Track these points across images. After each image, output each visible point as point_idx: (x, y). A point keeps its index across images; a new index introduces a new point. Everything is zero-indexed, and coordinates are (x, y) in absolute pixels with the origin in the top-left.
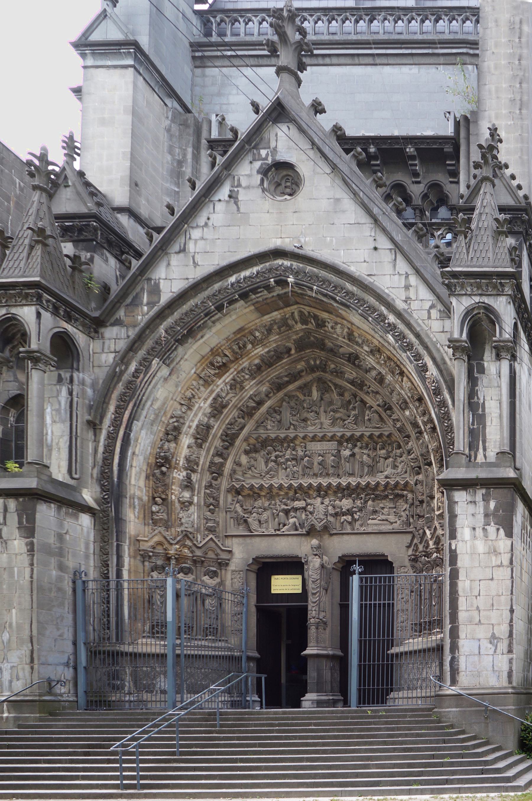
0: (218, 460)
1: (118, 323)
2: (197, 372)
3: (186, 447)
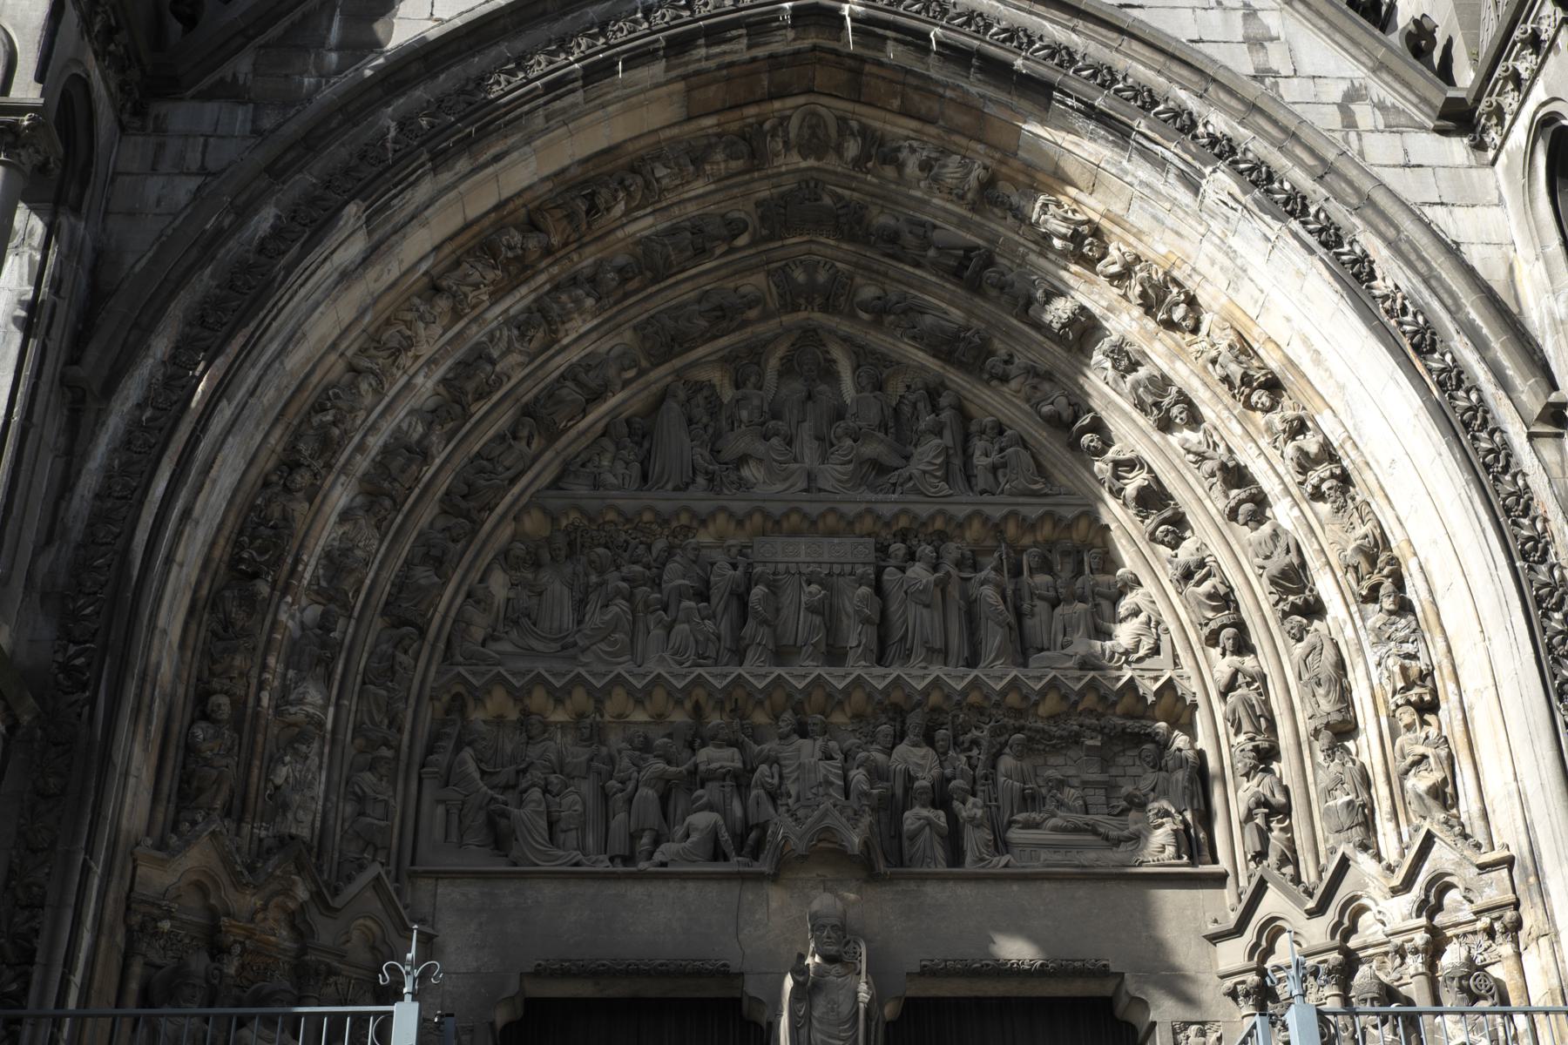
0: (424, 575)
1: (231, 92)
2: (434, 272)
3: (333, 518)
